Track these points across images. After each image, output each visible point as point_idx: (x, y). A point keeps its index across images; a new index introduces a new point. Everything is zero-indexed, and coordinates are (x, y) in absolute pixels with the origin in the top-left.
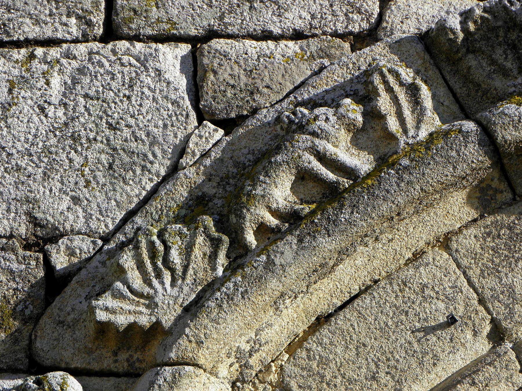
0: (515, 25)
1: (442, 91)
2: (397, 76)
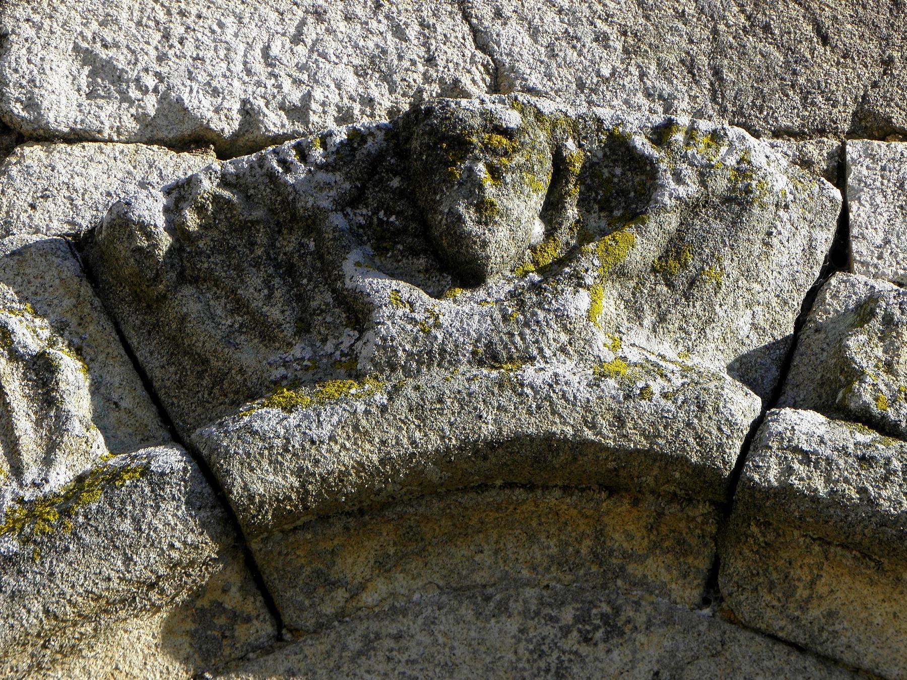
0: (294, 218)
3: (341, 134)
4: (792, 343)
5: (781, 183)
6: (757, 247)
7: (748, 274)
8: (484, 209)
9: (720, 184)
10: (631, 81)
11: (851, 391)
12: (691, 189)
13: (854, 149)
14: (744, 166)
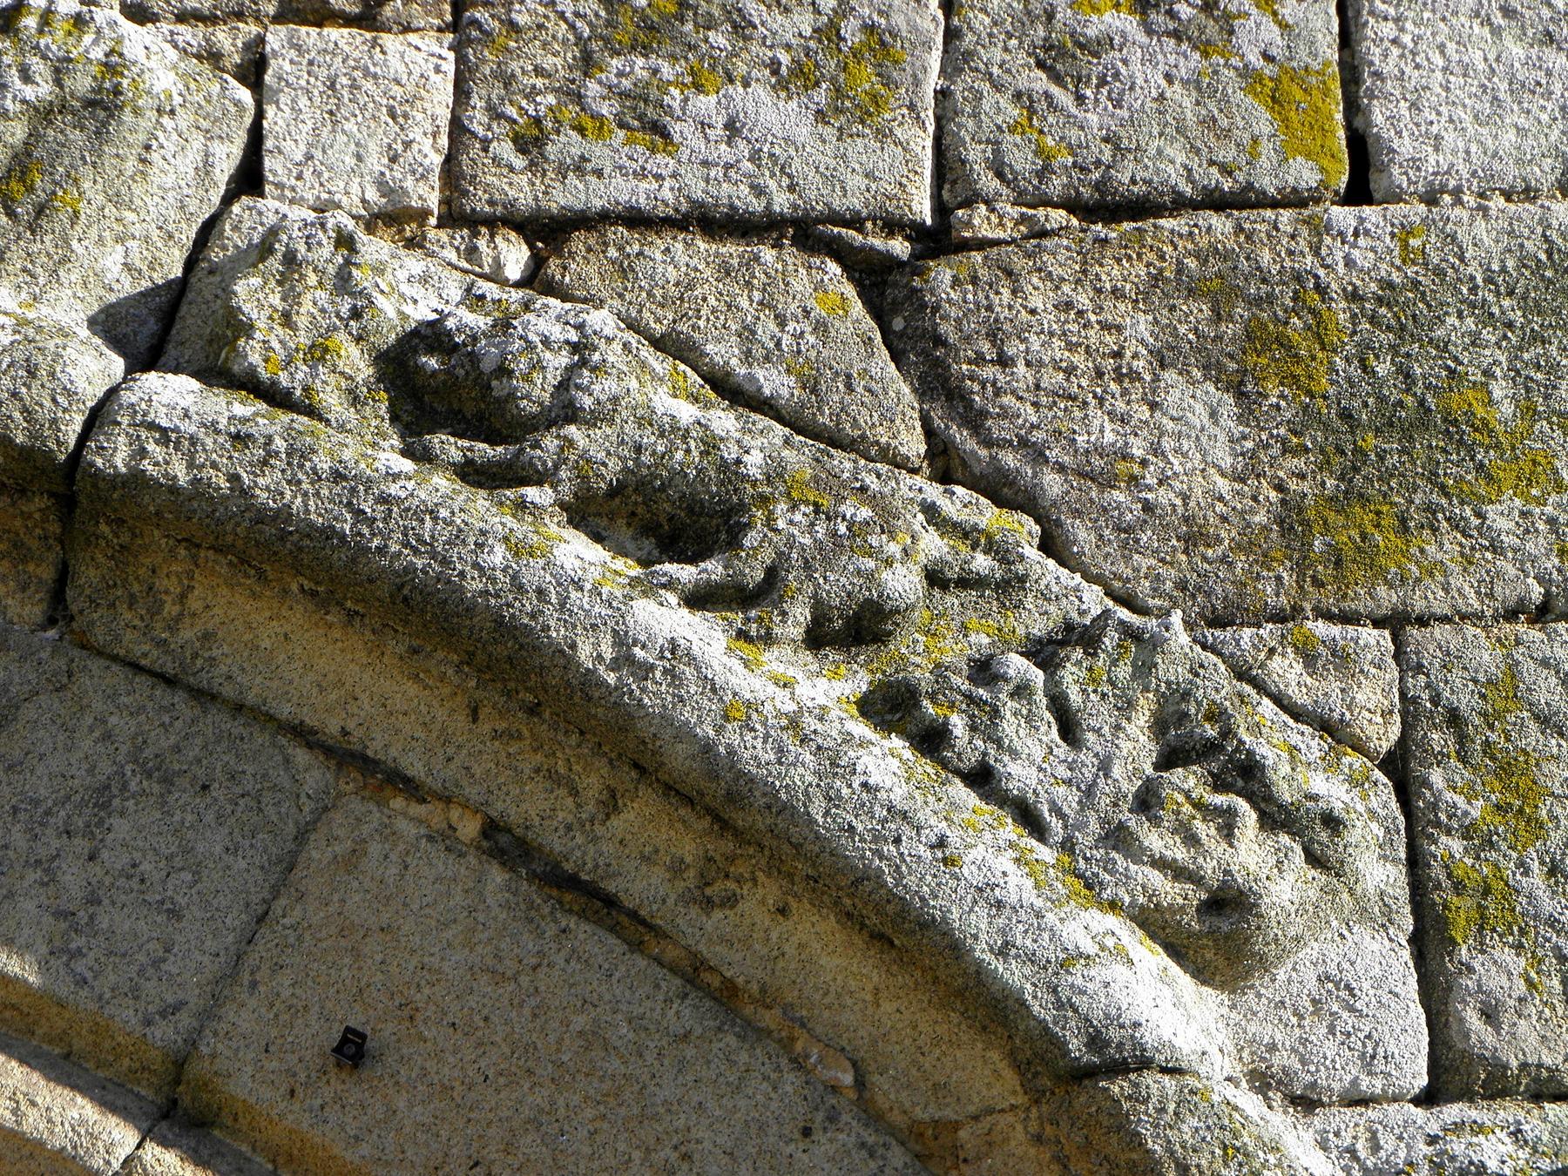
4: (177, 291)
6: (131, 165)
7: (116, 199)
9: (81, 83)
11: (235, 349)
12: (42, 90)
13: (276, 38)
14: (114, 59)
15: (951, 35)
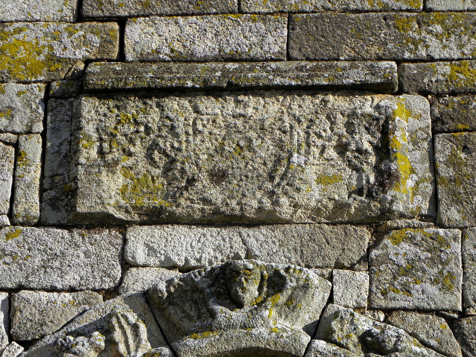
0: (197, 289)
1: (154, 327)
2: (126, 319)
3: (209, 269)
4: (319, 322)
5: (316, 282)
6: (310, 299)
7: (308, 305)
8: (244, 289)
9: (301, 283)
10: (281, 253)
11: (332, 336)
12: (294, 284)
14: (307, 278)
15: (464, 273)
